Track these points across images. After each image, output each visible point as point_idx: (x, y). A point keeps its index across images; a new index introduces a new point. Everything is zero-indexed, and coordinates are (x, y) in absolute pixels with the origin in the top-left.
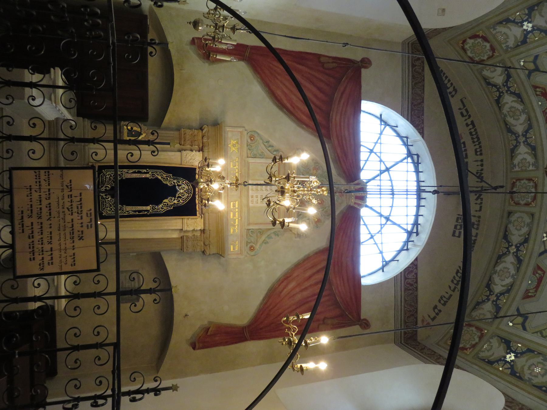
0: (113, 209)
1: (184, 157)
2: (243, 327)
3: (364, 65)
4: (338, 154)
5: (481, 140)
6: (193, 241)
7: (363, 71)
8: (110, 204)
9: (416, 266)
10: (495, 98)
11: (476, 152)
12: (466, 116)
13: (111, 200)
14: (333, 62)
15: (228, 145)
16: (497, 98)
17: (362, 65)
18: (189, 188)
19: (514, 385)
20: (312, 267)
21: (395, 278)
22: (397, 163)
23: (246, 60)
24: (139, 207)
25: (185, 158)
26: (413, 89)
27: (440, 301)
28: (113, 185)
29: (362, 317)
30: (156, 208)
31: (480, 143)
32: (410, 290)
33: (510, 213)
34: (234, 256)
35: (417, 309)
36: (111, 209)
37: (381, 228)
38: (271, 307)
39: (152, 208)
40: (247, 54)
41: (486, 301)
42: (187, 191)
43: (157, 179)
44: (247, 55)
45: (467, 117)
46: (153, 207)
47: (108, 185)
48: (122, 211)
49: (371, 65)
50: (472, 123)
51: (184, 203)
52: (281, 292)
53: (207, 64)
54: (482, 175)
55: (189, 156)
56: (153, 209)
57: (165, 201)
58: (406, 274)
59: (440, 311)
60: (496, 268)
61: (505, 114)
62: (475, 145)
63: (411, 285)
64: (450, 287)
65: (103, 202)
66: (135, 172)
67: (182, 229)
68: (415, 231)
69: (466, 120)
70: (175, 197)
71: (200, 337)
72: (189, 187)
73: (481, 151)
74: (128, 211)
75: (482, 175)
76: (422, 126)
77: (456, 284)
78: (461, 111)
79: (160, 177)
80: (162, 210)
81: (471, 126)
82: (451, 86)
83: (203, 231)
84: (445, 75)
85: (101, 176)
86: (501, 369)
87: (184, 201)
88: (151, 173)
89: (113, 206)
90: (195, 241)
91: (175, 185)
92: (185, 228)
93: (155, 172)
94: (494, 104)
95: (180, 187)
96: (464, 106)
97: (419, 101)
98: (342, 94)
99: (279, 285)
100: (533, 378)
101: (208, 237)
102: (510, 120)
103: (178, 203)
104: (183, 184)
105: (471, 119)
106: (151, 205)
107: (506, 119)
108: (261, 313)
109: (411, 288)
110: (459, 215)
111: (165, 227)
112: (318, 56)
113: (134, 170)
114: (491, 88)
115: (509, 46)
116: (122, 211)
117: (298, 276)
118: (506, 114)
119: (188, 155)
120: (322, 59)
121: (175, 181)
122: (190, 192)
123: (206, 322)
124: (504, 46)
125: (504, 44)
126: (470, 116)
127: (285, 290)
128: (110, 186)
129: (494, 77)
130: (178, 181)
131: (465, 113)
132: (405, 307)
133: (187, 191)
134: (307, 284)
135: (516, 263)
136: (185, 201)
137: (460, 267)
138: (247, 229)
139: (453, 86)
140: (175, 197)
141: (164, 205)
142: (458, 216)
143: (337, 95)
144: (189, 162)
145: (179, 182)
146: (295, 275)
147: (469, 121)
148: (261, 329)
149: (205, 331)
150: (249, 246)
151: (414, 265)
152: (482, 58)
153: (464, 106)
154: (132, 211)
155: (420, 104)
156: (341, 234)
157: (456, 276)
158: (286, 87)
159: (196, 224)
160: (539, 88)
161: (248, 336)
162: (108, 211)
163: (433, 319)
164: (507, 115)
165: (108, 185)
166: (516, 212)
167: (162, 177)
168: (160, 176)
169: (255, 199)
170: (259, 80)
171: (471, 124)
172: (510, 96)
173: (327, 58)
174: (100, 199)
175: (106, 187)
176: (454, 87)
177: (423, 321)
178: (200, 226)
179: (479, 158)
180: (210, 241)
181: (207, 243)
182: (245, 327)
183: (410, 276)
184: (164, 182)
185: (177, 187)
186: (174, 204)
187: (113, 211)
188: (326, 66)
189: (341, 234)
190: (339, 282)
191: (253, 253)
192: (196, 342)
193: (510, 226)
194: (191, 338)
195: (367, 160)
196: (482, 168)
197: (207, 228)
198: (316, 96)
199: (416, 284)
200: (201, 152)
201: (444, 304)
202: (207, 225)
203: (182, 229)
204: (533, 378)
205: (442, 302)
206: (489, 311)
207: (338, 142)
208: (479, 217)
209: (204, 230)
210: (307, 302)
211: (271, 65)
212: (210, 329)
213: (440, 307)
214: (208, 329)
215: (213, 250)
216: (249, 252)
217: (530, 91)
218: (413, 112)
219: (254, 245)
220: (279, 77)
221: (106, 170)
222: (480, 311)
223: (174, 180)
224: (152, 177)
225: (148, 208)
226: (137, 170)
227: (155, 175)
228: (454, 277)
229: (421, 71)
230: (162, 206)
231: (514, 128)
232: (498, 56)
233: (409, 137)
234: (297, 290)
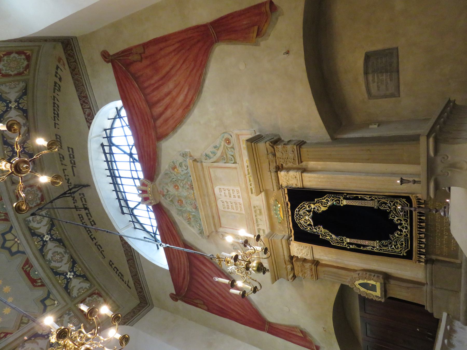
0: (392, 205)
1: (310, 254)
2: (218, 42)
4: (174, 229)
6: (288, 158)
8: (396, 211)
9: (87, 122)
10: (76, 265)
13: (394, 217)
14: (197, 303)
16: (75, 265)
18: (299, 221)
20: (166, 121)
21: (98, 110)
23: (267, 322)
24: (357, 204)
25: (309, 252)
26: (137, 271)
28: (391, 236)
30: (335, 201)
34: (244, 132)
36: (394, 205)
38: (195, 71)
39: (339, 202)
41: (18, 100)
42: (301, 217)
44: (266, 325)
46: (339, 203)
47: (398, 236)
48: (379, 201)
49: (170, 295)
51: (303, 204)
52: (189, 90)
55: (304, 253)
56: (339, 201)
57: (326, 208)
58: (91, 114)
60: (26, 128)
61: (66, 254)
65: (405, 215)
66: (364, 246)
67: (302, 173)
70: (314, 212)
71: (266, 21)
72: (298, 222)
74: (372, 200)
80: (327, 198)
83: (279, 169)
85: (408, 248)
87: (304, 206)
88: (344, 243)
89: (392, 209)
90: (285, 158)
91: (315, 226)
92: (298, 174)
93: (340, 243)
95: (308, 223)
99: (192, 98)
101: (270, 162)
102: (61, 250)
103: (310, 204)
104: (306, 226)
106: (342, 205)
107: (65, 250)
108: (203, 63)
111: (322, 177)
112: (208, 310)
113: (365, 249)
114: (81, 273)
115: (67, 315)
116: (379, 201)
117: (178, 110)
118: (65, 254)
119: (305, 254)
120: (206, 308)
121: (315, 231)
122: (297, 215)
123: (263, 43)
124: (72, 314)
125: (72, 316)
127: (185, 93)
128: (396, 235)
129: (80, 283)
130: (312, 230)
132: (81, 78)
133: (301, 217)
134: (167, 100)
136: (301, 205)
137: (58, 120)
138: (236, 163)
140: (314, 211)
141: (326, 204)
144: (303, 247)
145: (310, 229)
146: (180, 111)
148: (198, 41)
149: (261, 32)
150: (231, 145)
151: (88, 122)
152: (90, 298)
153: (101, 252)
154: (367, 200)
159: (287, 178)
161: (210, 29)
162: (399, 202)
164: (64, 253)
165: (398, 237)
167: (331, 236)
168: (332, 237)
169: (236, 194)
170: (252, 303)
172: (63, 271)
174: (409, 220)
175: (401, 235)
178: (282, 174)
180: (268, 158)
181: (270, 156)
182: (216, 42)
184: (328, 231)
185: (312, 224)
186: (314, 204)
187: (392, 202)
188: (202, 302)
190: (140, 103)
191: (226, 136)
192: (269, 12)
194: (277, 19)
197: (273, 174)
200: (292, 255)
202: (273, 178)
203: (302, 173)
206: (10, 92)
207: (177, 240)
209: (276, 172)
210: (162, 79)
212: (255, 34)
214: (258, 35)
215: (262, 146)
216: (230, 137)
217: (47, 281)
219: (227, 145)
220: (236, 302)
221: (402, 255)
222: (16, 90)
223: (316, 232)
224: (342, 238)
225: (345, 202)
226: (362, 248)
227: (339, 239)
230: (328, 203)
231: (56, 245)
233: (134, 229)
234: (174, 93)
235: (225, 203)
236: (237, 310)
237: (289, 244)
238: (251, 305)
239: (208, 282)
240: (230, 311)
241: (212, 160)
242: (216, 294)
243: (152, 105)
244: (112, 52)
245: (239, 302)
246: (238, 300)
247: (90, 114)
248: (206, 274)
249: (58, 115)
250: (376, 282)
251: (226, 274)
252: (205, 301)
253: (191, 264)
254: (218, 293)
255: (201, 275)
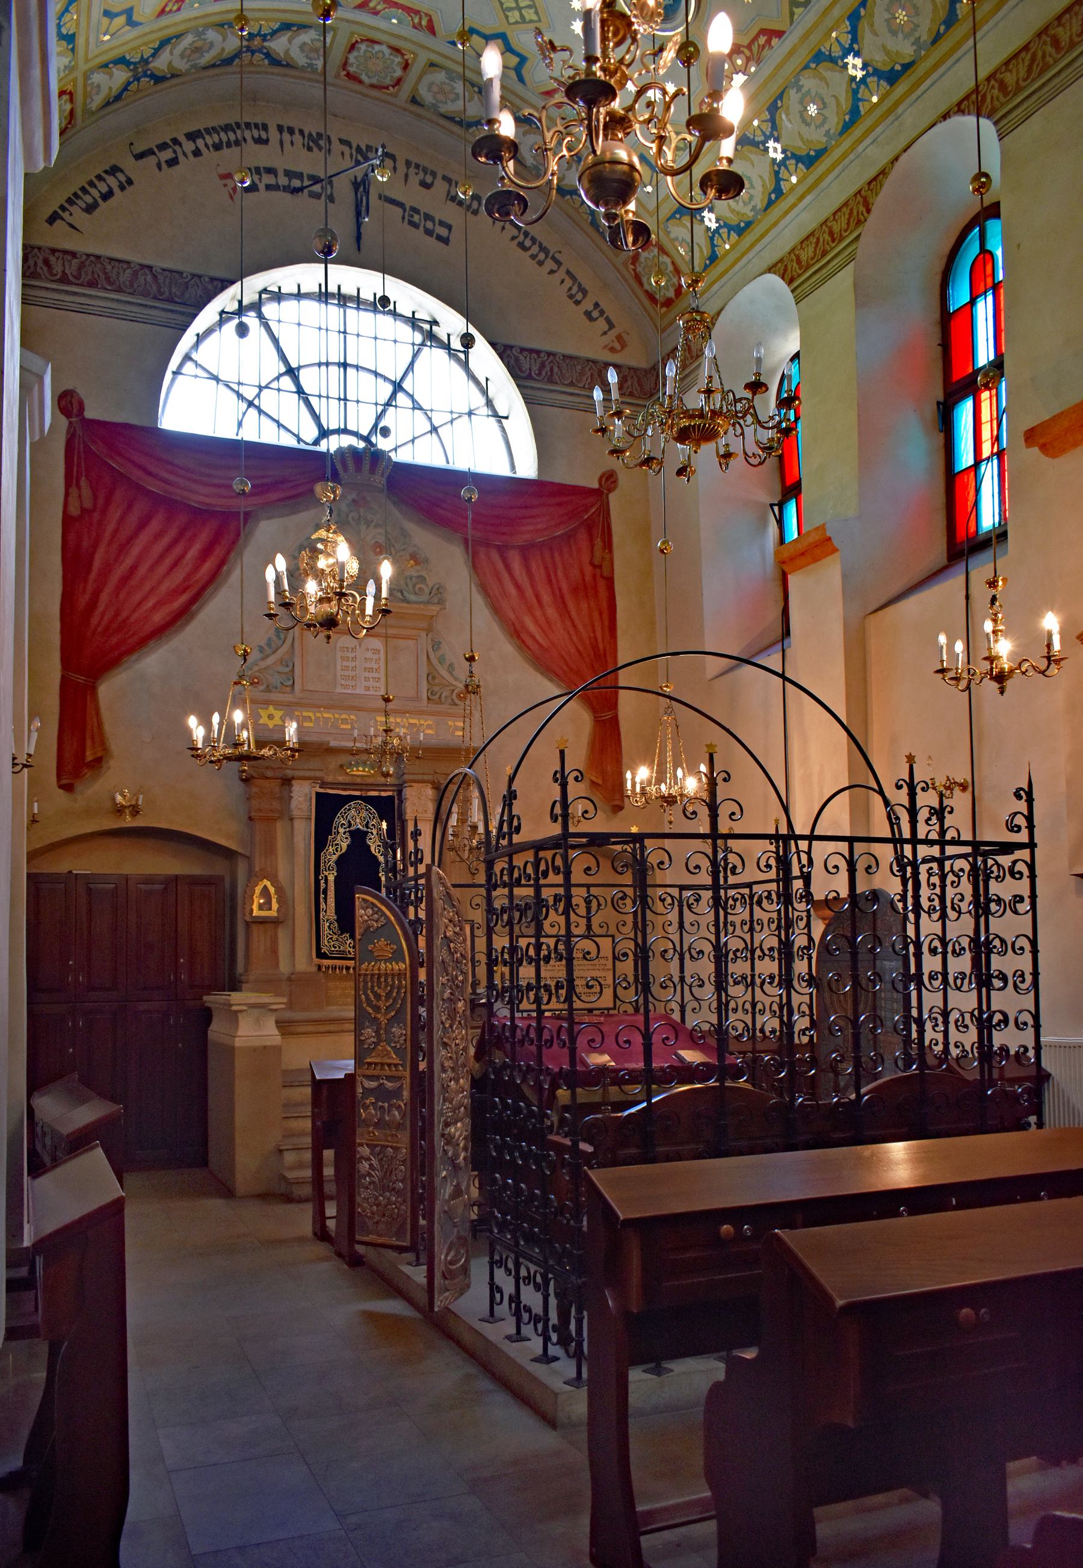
3: (75, 411)
5: (232, 122)
7: (89, 414)
11: (259, 141)
12: (175, 152)
14: (78, 487)
15: (270, 730)
17: (77, 416)
19: (759, 240)
22: (275, 341)
26: (119, 290)
27: (577, 303)
29: (596, 486)
31: (238, 125)
32: (552, 369)
33: (414, 101)
35: (588, 360)
37: (421, 409)
40: (81, 679)
43: (337, 862)
45: (177, 148)
50: (192, 136)
53: (112, 763)
54: (315, 135)
59: (597, 305)
62: (245, 140)
63: (543, 365)
64: (552, 272)
68: (427, 327)
69: (185, 154)
73: (256, 126)
75: (315, 135)
76: (207, 279)
77: (546, 257)
78: (164, 166)
79: (335, 858)
81: (200, 143)
82: (104, 180)
84: (80, 193)
86: (727, 247)
94: (160, 86)
96: (151, 152)
97: (149, 278)
98: (150, 474)
100: (753, 203)
102: (207, 58)
105: (182, 139)
109: (548, 368)
110: (403, 218)
112: (68, 521)
120: (74, 511)
126: (175, 141)
131: (168, 154)
135: (527, 127)
139: (104, 175)
142: (406, 220)
143: (153, 486)
147: (189, 146)
153: (151, 152)
155: (155, 277)
156: (442, 512)
157: (530, 253)
158: (145, 599)
160: (166, 5)
163: (611, 326)
166: (415, 89)
170: (134, 657)
171: (194, 142)
173: (70, 498)
176: (106, 172)
177: (612, 350)
179: (274, 135)
183: (526, 366)
188: (88, 504)
189: (442, 512)
190: (530, 528)
193: (444, 109)
195: (277, 422)
196: (297, 132)
198: (158, 536)
199: (542, 355)
201: (585, 293)
204: (753, 203)
205: (579, 296)
208: (408, 163)
211: (100, 629)
213: (588, 305)
217: (165, 21)
218: (177, 299)
220: (124, 614)
228: (533, 257)
229: (75, 260)
232: (75, 85)
233: (220, 309)
235: (353, 655)
236: (101, 607)
237: (314, 779)
238: (131, 651)
239: (158, 548)
240: (90, 588)
241: (430, 650)
242: (129, 562)
243: (525, 551)
244: (613, 498)
245: (124, 621)
246: (132, 619)
247: (520, 369)
248: (178, 550)
249: (521, 245)
250: (278, 910)
251: (194, 608)
252: (96, 516)
253: (199, 515)
254: (133, 569)
255: (172, 533)
